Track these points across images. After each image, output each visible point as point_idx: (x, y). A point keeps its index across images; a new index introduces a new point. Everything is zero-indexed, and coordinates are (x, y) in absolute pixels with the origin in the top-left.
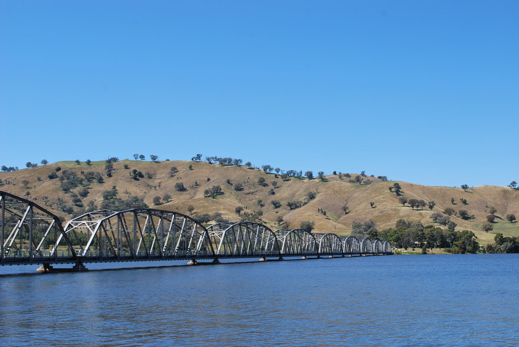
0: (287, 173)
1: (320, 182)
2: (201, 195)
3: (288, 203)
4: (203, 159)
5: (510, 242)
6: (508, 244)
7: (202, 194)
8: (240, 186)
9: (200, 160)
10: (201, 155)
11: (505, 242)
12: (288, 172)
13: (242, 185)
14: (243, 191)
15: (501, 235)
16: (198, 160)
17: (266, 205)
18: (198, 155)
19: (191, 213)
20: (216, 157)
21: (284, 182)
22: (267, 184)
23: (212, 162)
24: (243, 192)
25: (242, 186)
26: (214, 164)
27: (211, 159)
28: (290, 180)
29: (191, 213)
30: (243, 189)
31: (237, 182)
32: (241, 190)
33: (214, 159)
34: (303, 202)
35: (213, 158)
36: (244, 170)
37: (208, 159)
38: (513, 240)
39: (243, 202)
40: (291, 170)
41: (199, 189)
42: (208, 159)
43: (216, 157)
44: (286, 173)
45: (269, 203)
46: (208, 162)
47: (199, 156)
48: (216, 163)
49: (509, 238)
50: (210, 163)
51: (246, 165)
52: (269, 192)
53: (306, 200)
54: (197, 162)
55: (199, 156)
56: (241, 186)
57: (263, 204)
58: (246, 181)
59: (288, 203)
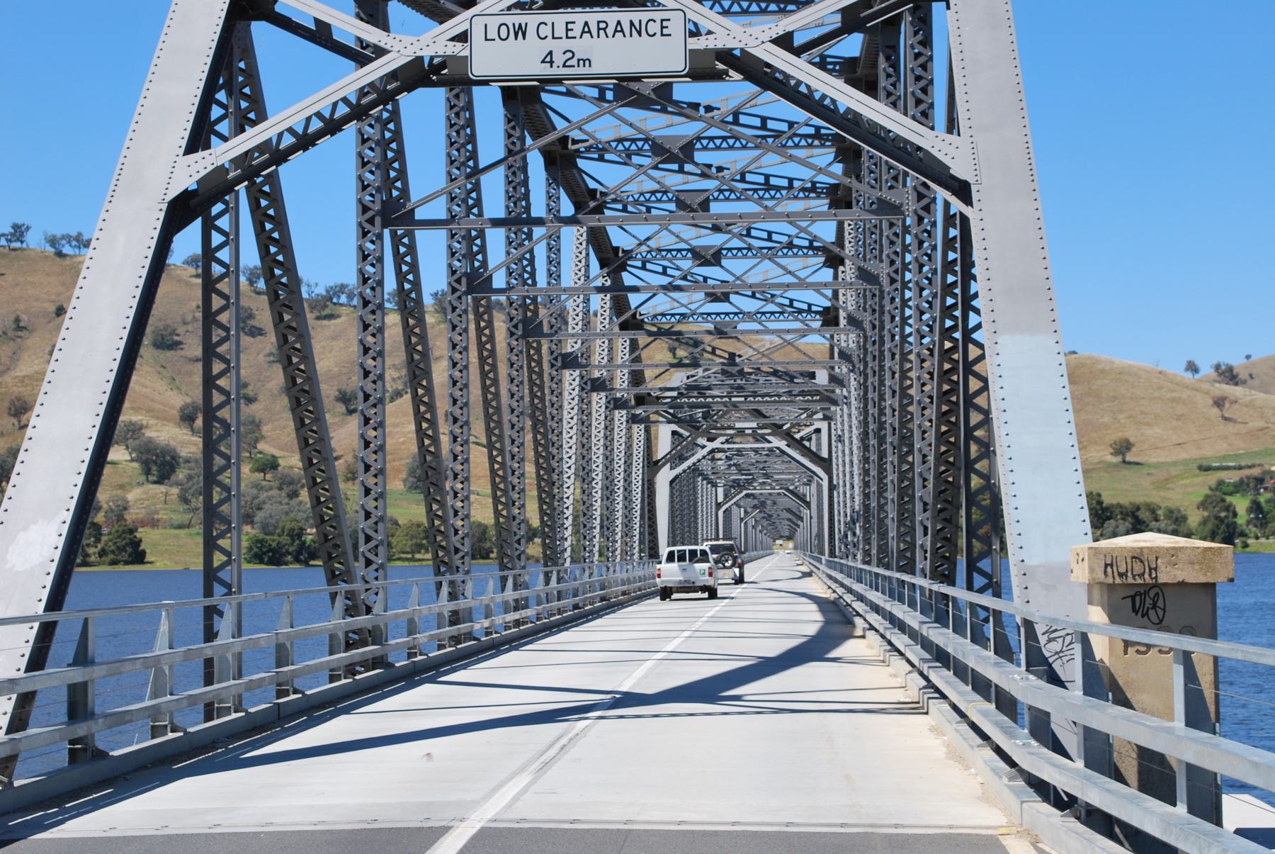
0: (328, 292)
1: (439, 323)
2: (36, 362)
3: (340, 391)
4: (34, 240)
5: (1124, 519)
6: (1117, 527)
7: (42, 360)
8: (171, 334)
9: (24, 245)
10: (28, 228)
11: (1109, 518)
12: (332, 288)
13: (177, 332)
14: (182, 349)
15: (1098, 498)
16: (17, 245)
17: (261, 397)
18: (16, 227)
19: (19, 421)
20: (80, 234)
21: (319, 322)
22: (261, 329)
23: (67, 250)
24: (182, 353)
25: (178, 335)
26: (72, 257)
27: (64, 242)
28: (339, 316)
29: (19, 421)
30: (180, 343)
31: (160, 320)
32: (174, 345)
33: (74, 243)
34: (390, 390)
35: (68, 238)
36: (179, 281)
37: (53, 241)
38: (1133, 513)
39: (184, 389)
40: (339, 282)
41: (29, 342)
42: (53, 241)
43: (80, 234)
44: (324, 293)
45: (271, 390)
46: (52, 250)
47: (19, 232)
48: (80, 255)
49: (1121, 507)
50: (60, 254)
51: (187, 262)
52: (269, 355)
53: (399, 382)
54: (15, 250)
55: (19, 232)
56: (174, 333)
57: (251, 394)
58: (189, 318)
59: (340, 391)
